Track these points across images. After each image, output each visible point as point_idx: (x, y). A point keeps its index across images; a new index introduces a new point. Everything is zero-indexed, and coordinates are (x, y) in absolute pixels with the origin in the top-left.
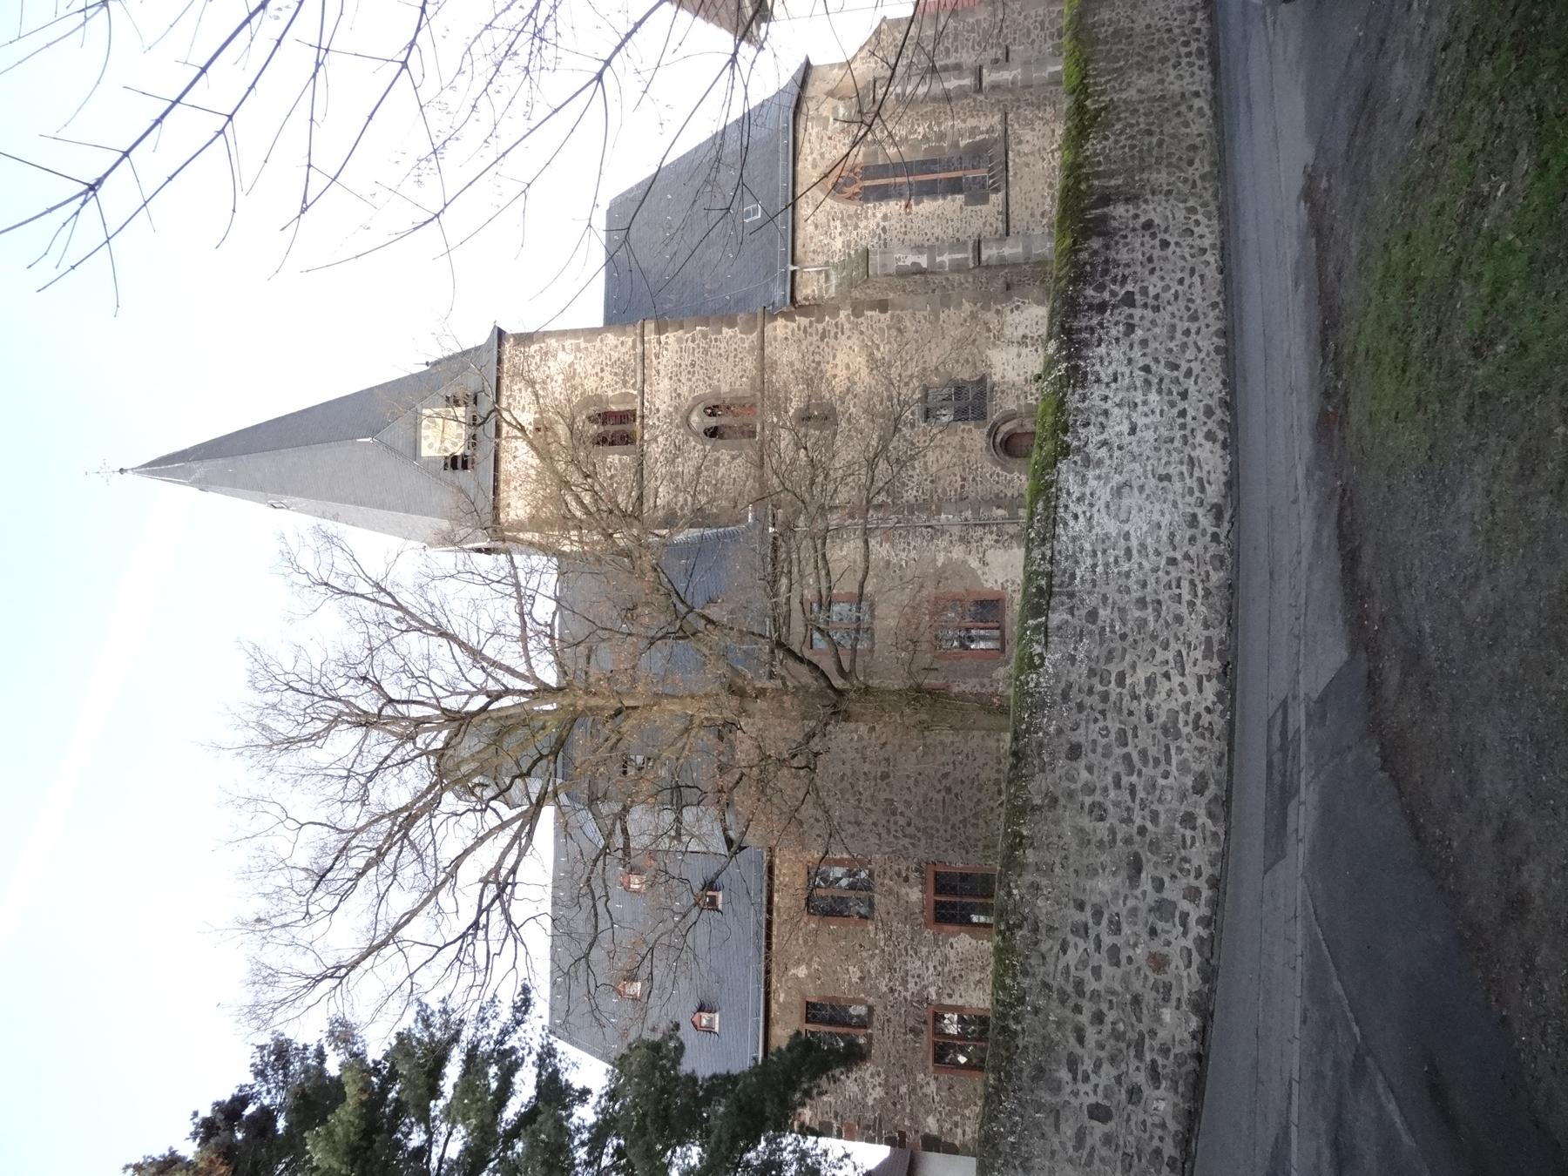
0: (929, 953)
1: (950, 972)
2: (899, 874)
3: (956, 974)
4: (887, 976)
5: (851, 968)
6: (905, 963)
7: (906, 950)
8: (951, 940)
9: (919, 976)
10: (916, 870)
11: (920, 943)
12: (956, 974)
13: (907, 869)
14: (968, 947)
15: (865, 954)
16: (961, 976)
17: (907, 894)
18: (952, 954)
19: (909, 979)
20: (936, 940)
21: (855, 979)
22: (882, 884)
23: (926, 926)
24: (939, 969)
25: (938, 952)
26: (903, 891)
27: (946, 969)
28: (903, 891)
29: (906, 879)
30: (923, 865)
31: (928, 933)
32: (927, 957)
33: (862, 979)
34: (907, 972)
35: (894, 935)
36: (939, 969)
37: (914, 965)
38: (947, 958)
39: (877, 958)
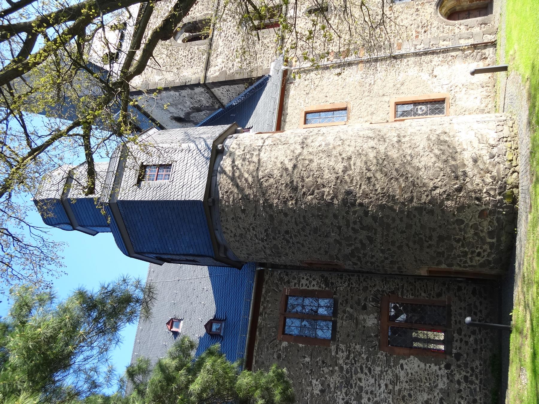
0: (382, 372)
1: (400, 391)
2: (358, 303)
3: (406, 393)
4: (344, 391)
5: (314, 382)
6: (360, 380)
7: (361, 369)
8: (401, 361)
9: (372, 392)
10: (373, 300)
11: (374, 362)
12: (406, 393)
13: (366, 299)
14: (417, 369)
15: (326, 370)
16: (410, 395)
17: (364, 320)
18: (402, 374)
19: (364, 395)
20: (388, 361)
21: (317, 392)
22: (344, 312)
23: (380, 348)
24: (390, 387)
25: (389, 372)
26: (361, 317)
27: (397, 388)
28: (361, 317)
29: (365, 308)
30: (379, 296)
31: (381, 355)
32: (380, 376)
33: (322, 391)
34: (361, 388)
35: (352, 355)
36: (390, 387)
37: (367, 382)
38: (397, 377)
39: (337, 374)
